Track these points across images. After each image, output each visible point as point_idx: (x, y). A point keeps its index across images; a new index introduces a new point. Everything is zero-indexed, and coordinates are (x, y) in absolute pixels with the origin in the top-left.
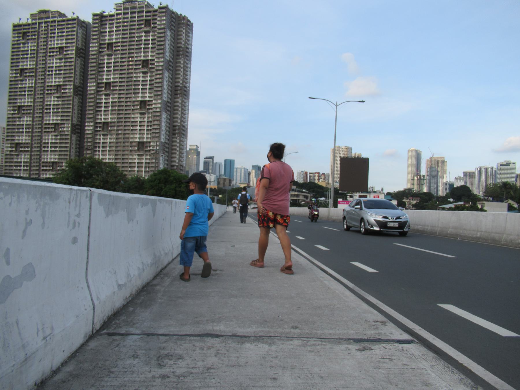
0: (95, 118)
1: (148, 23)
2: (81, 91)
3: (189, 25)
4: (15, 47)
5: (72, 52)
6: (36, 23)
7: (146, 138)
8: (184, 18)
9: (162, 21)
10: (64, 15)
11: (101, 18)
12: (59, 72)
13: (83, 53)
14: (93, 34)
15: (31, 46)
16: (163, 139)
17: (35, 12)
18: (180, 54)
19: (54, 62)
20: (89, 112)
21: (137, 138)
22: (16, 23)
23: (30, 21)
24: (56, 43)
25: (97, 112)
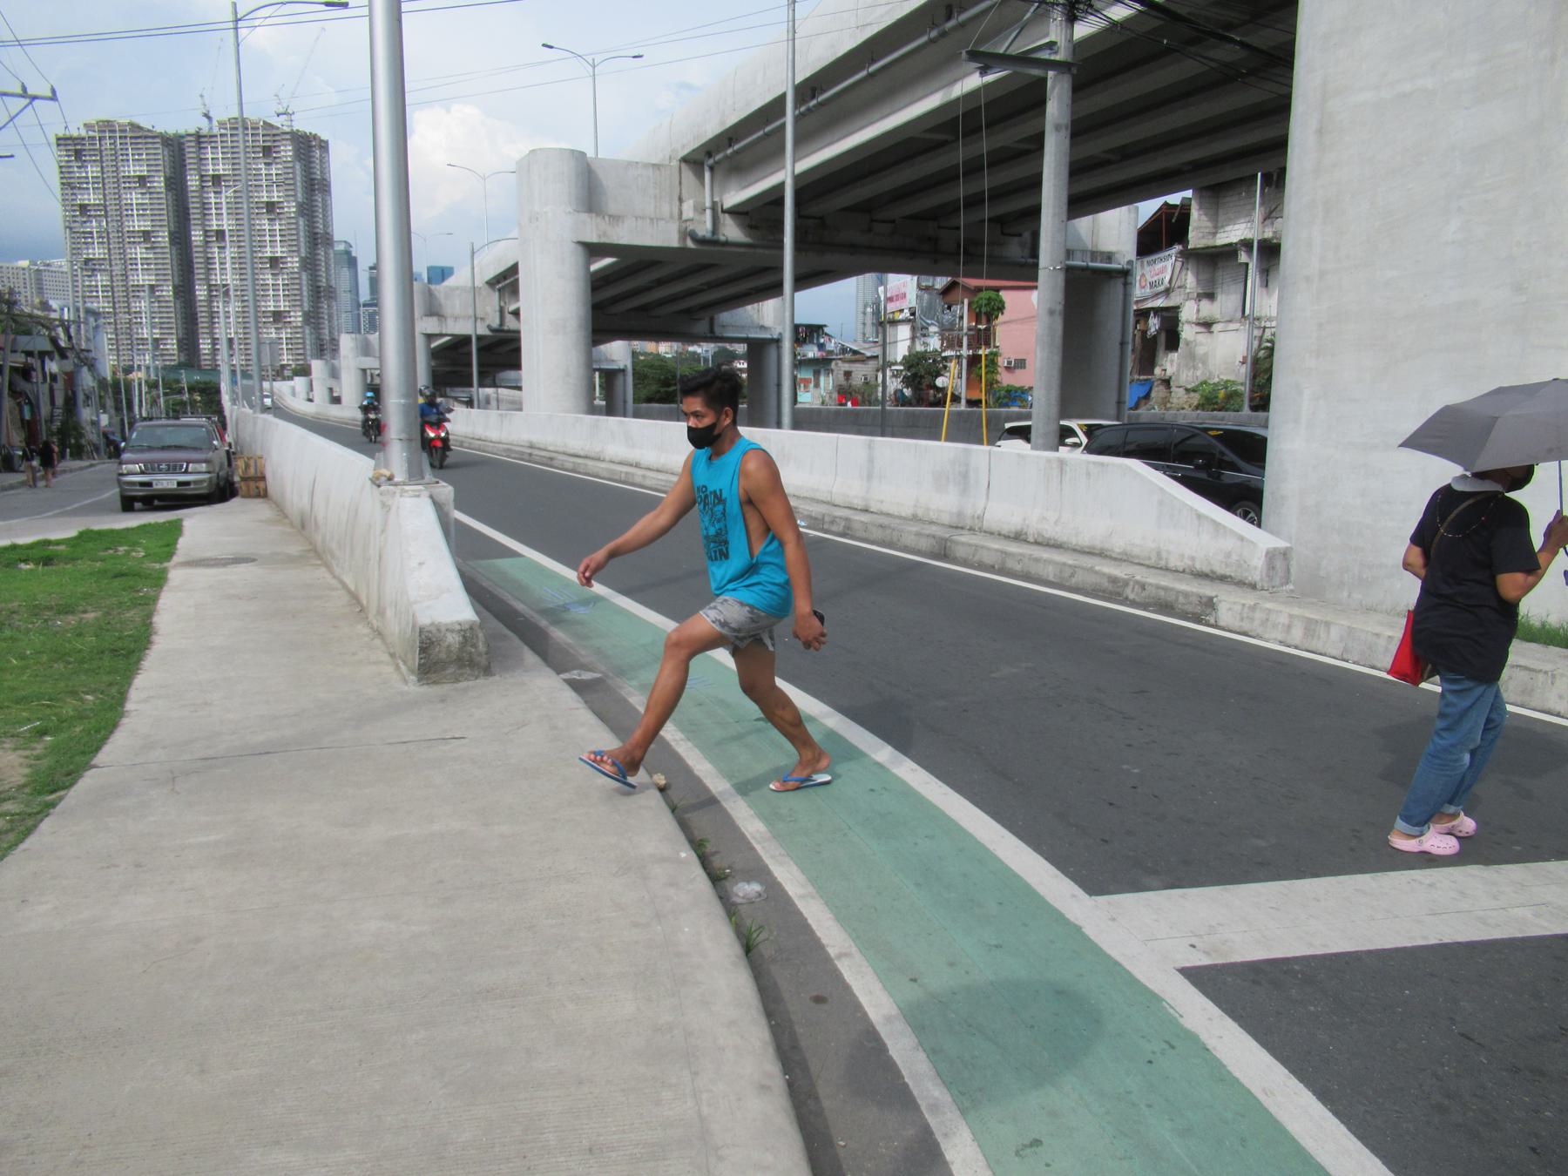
0: (207, 279)
1: (267, 151)
2: (180, 238)
3: (324, 146)
4: (64, 170)
5: (159, 183)
6: (93, 138)
7: (283, 306)
8: (315, 137)
9: (287, 151)
10: (140, 128)
11: (198, 137)
12: (143, 212)
13: (176, 183)
14: (190, 160)
15: (92, 171)
16: (306, 307)
17: (92, 119)
18: (315, 187)
19: (134, 197)
20: (199, 272)
21: (271, 306)
22: (61, 135)
23: (83, 133)
24: (133, 170)
25: (209, 271)
